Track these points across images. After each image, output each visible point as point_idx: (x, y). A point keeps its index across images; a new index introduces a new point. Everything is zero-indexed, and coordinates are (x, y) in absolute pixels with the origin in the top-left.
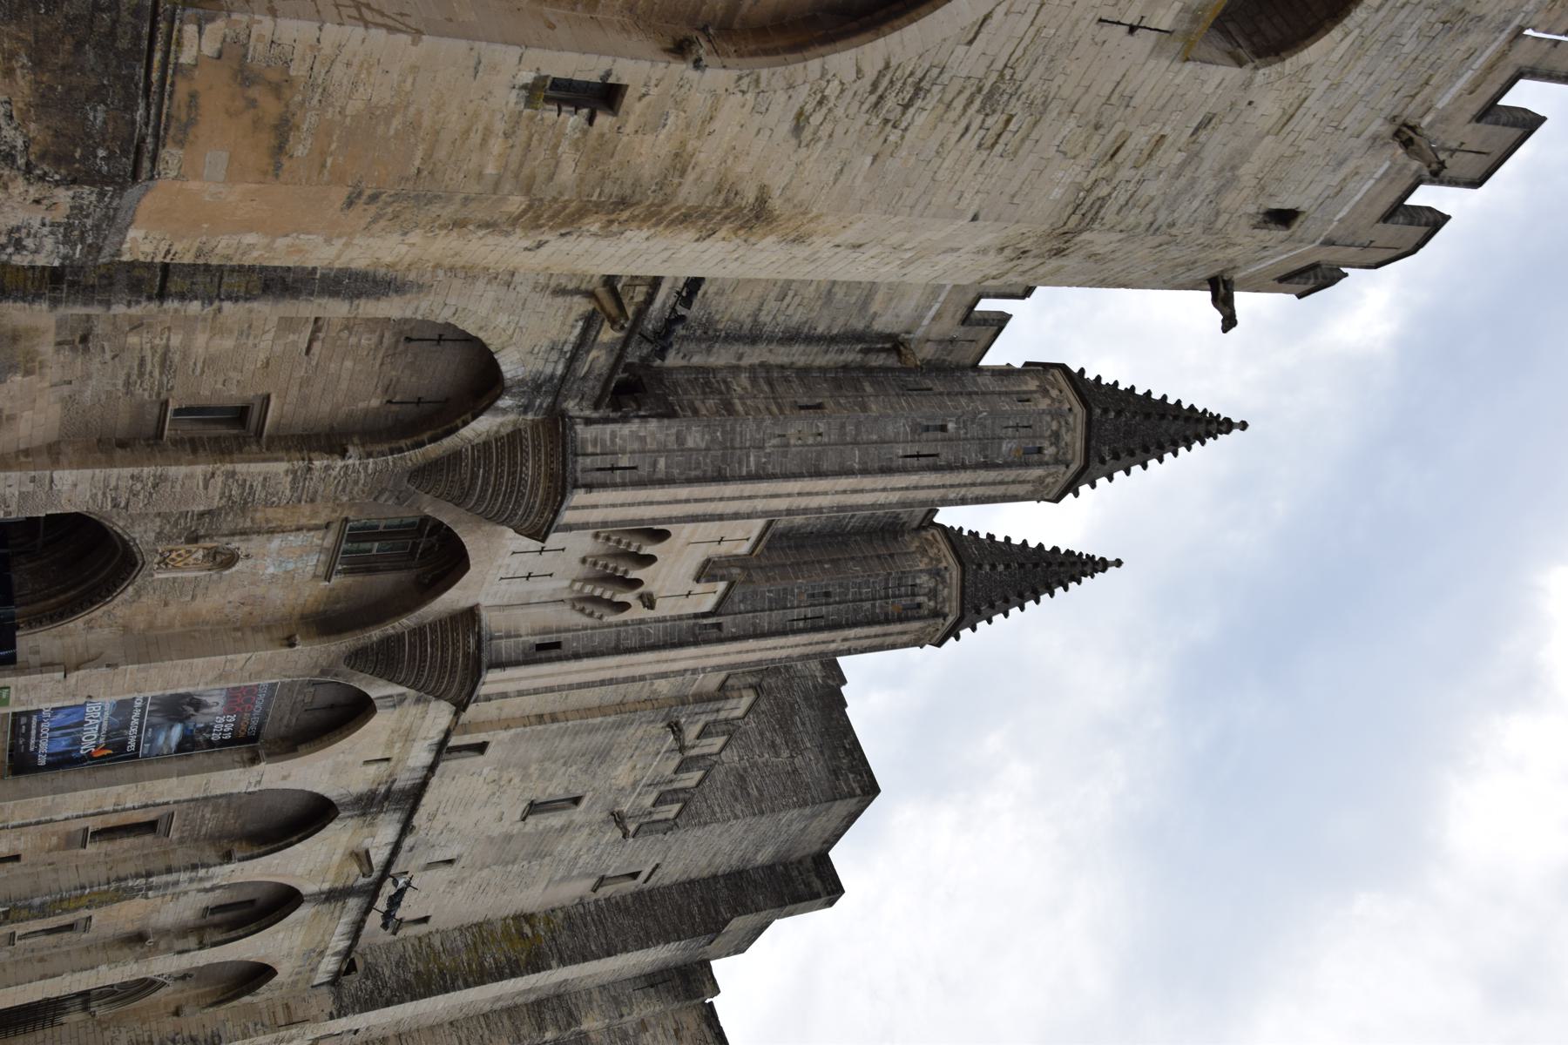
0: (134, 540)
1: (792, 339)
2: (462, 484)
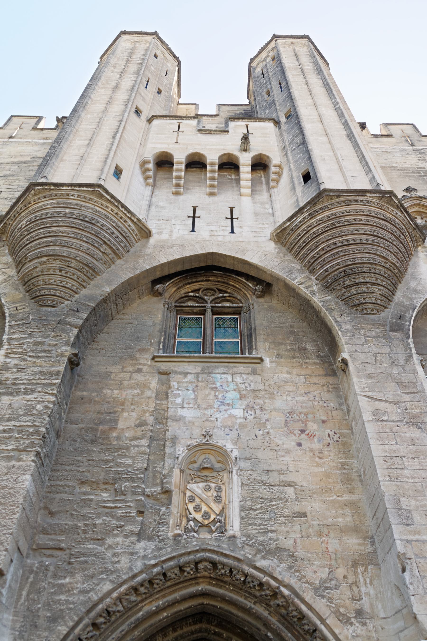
0: (147, 568)
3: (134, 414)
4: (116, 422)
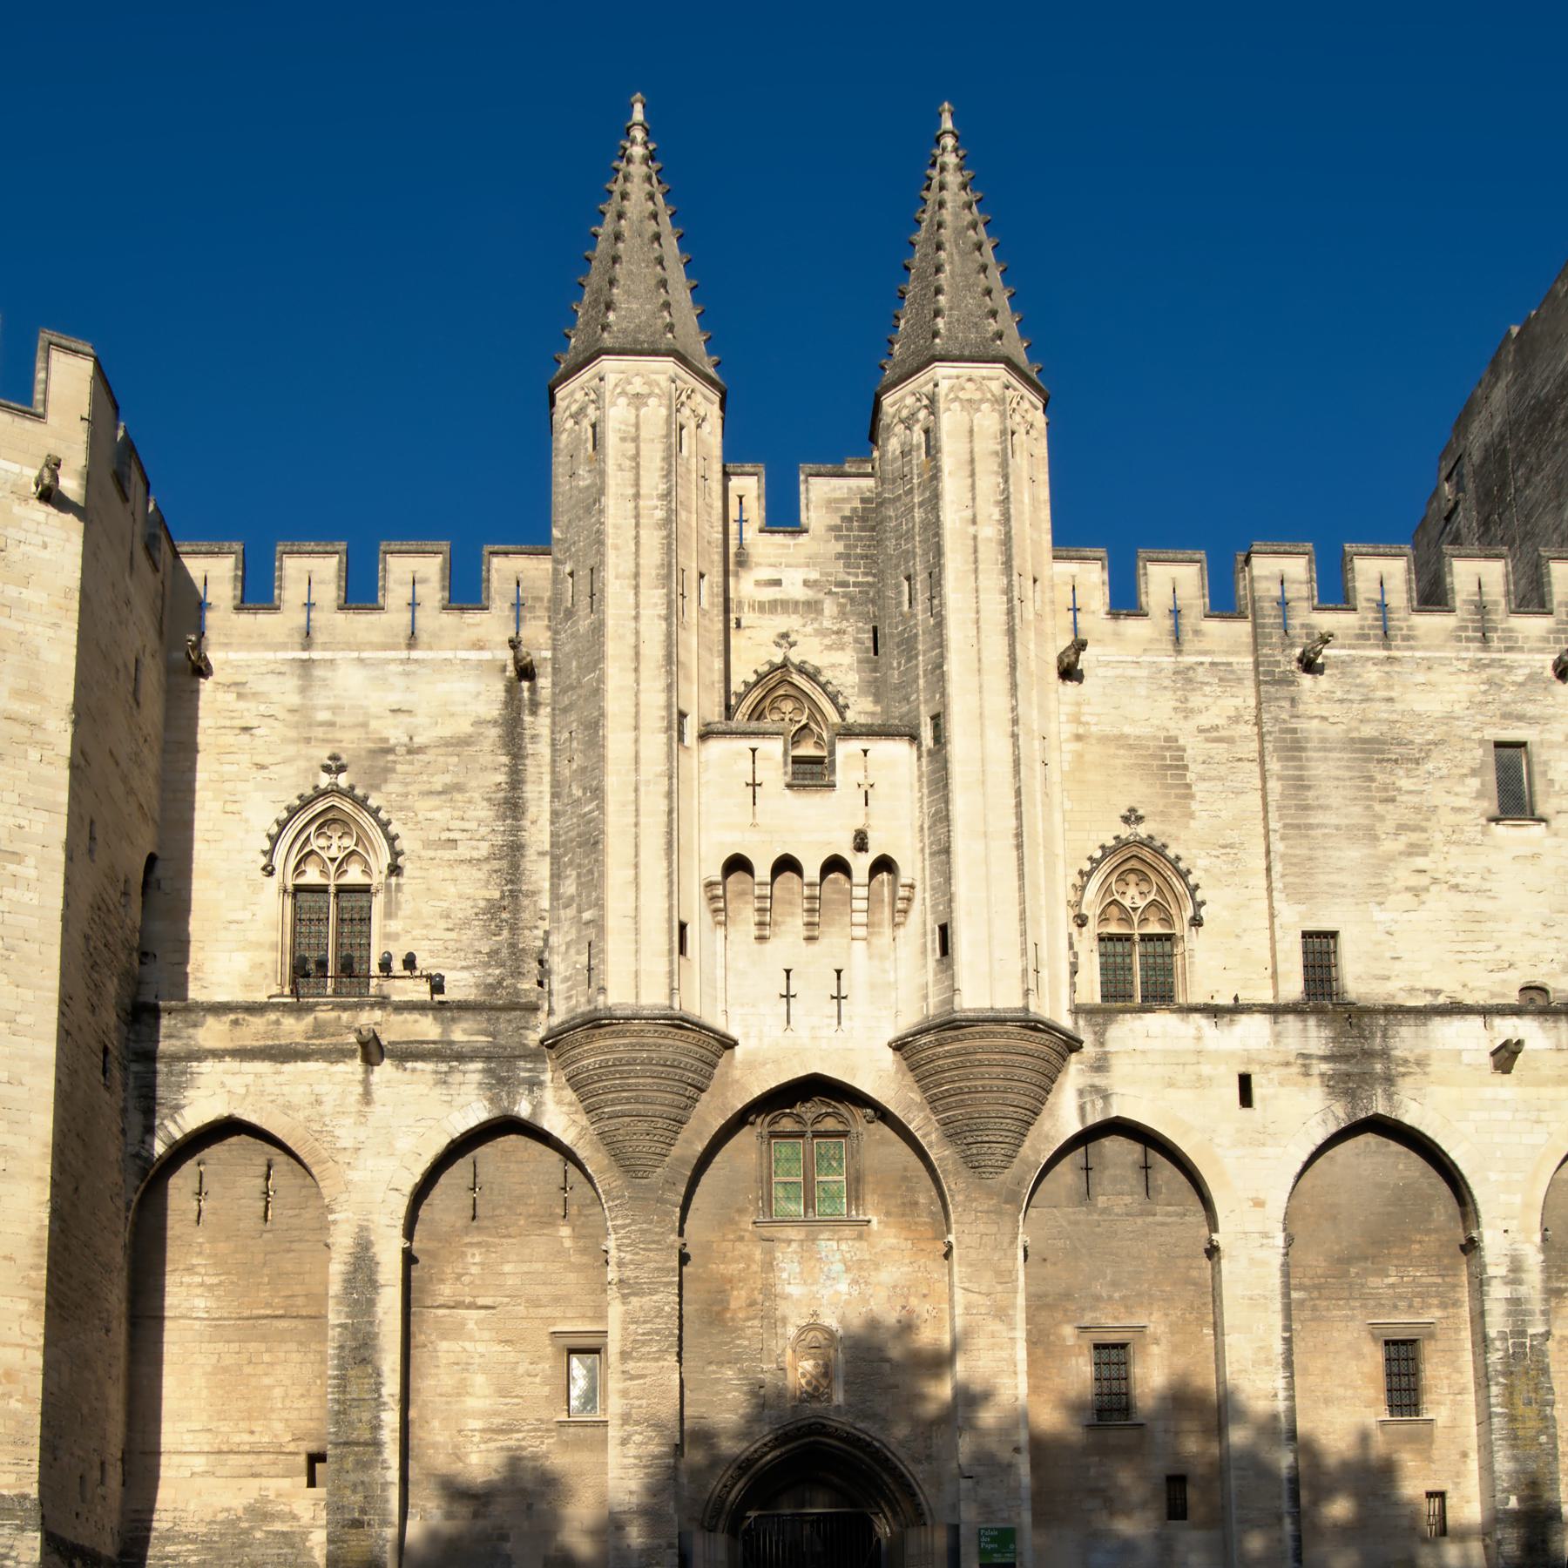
1: (516, 805)
2: (629, 1125)
3: (743, 1293)
4: (728, 1303)
